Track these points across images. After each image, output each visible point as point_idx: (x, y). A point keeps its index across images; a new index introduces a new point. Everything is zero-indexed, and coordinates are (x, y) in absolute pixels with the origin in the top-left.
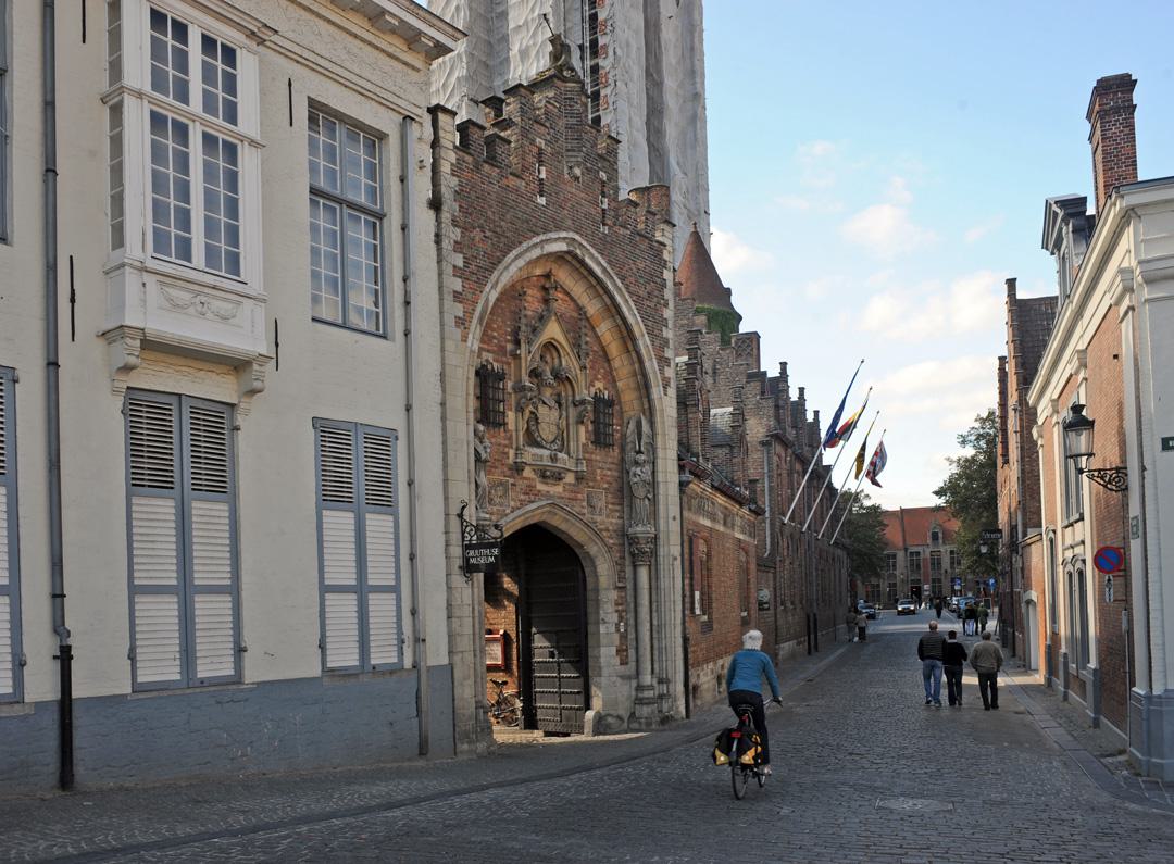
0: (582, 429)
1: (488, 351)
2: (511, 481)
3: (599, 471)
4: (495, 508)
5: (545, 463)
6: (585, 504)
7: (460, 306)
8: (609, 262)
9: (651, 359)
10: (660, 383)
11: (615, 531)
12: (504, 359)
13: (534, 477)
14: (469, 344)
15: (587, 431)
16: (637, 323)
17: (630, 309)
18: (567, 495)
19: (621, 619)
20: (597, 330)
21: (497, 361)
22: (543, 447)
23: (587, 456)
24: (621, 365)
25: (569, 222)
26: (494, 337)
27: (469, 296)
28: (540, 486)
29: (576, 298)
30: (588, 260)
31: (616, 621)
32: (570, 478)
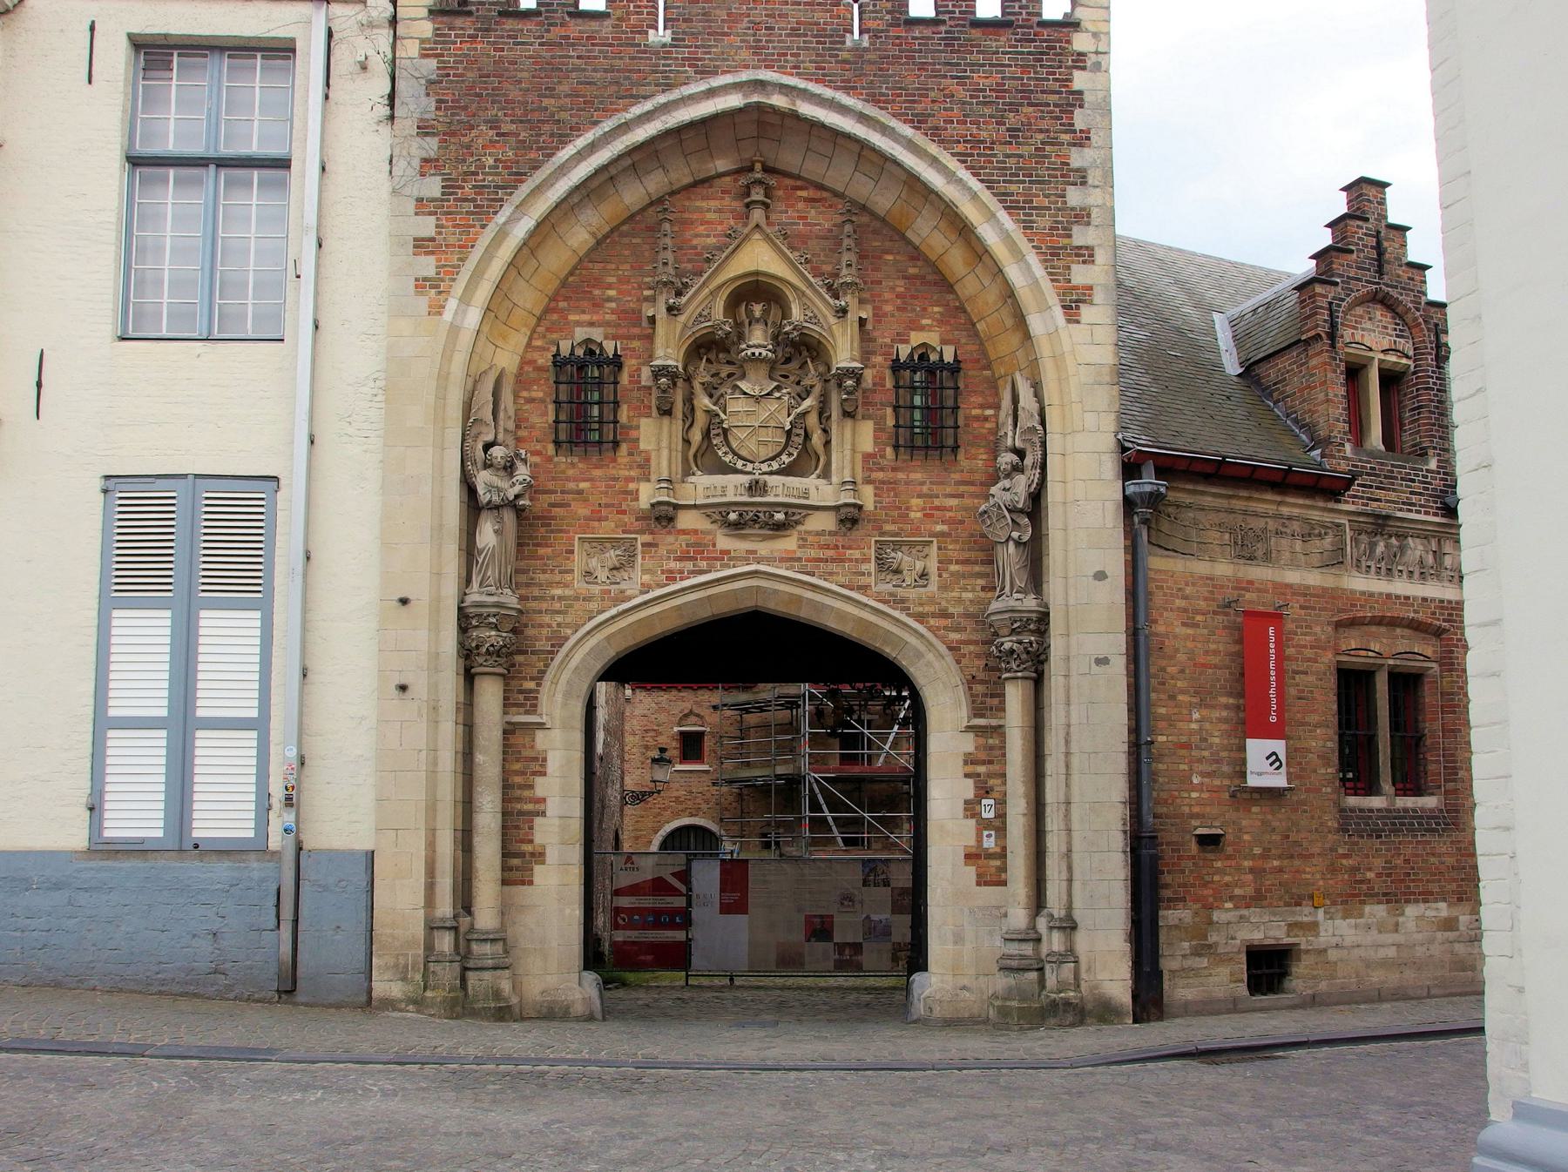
0: (866, 430)
1: (591, 324)
2: (641, 539)
3: (915, 502)
4: (596, 589)
5: (730, 498)
6: (872, 567)
7: (432, 259)
8: (874, 99)
9: (1019, 257)
10: (1053, 300)
11: (967, 615)
12: (636, 331)
13: (714, 527)
14: (448, 315)
15: (879, 429)
16: (974, 196)
17: (950, 176)
18: (813, 553)
19: (984, 791)
20: (909, 234)
21: (615, 338)
22: (737, 471)
23: (880, 475)
24: (971, 284)
25: (745, 55)
26: (610, 299)
27: (452, 240)
28: (724, 542)
29: (840, 188)
30: (807, 109)
31: (970, 795)
32: (823, 522)
